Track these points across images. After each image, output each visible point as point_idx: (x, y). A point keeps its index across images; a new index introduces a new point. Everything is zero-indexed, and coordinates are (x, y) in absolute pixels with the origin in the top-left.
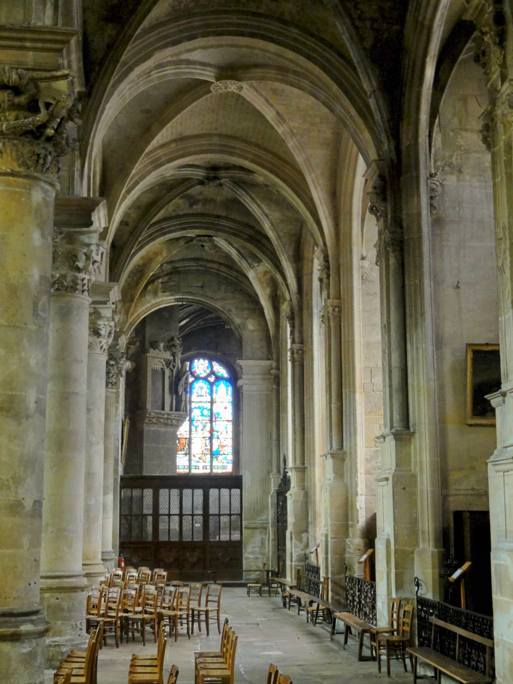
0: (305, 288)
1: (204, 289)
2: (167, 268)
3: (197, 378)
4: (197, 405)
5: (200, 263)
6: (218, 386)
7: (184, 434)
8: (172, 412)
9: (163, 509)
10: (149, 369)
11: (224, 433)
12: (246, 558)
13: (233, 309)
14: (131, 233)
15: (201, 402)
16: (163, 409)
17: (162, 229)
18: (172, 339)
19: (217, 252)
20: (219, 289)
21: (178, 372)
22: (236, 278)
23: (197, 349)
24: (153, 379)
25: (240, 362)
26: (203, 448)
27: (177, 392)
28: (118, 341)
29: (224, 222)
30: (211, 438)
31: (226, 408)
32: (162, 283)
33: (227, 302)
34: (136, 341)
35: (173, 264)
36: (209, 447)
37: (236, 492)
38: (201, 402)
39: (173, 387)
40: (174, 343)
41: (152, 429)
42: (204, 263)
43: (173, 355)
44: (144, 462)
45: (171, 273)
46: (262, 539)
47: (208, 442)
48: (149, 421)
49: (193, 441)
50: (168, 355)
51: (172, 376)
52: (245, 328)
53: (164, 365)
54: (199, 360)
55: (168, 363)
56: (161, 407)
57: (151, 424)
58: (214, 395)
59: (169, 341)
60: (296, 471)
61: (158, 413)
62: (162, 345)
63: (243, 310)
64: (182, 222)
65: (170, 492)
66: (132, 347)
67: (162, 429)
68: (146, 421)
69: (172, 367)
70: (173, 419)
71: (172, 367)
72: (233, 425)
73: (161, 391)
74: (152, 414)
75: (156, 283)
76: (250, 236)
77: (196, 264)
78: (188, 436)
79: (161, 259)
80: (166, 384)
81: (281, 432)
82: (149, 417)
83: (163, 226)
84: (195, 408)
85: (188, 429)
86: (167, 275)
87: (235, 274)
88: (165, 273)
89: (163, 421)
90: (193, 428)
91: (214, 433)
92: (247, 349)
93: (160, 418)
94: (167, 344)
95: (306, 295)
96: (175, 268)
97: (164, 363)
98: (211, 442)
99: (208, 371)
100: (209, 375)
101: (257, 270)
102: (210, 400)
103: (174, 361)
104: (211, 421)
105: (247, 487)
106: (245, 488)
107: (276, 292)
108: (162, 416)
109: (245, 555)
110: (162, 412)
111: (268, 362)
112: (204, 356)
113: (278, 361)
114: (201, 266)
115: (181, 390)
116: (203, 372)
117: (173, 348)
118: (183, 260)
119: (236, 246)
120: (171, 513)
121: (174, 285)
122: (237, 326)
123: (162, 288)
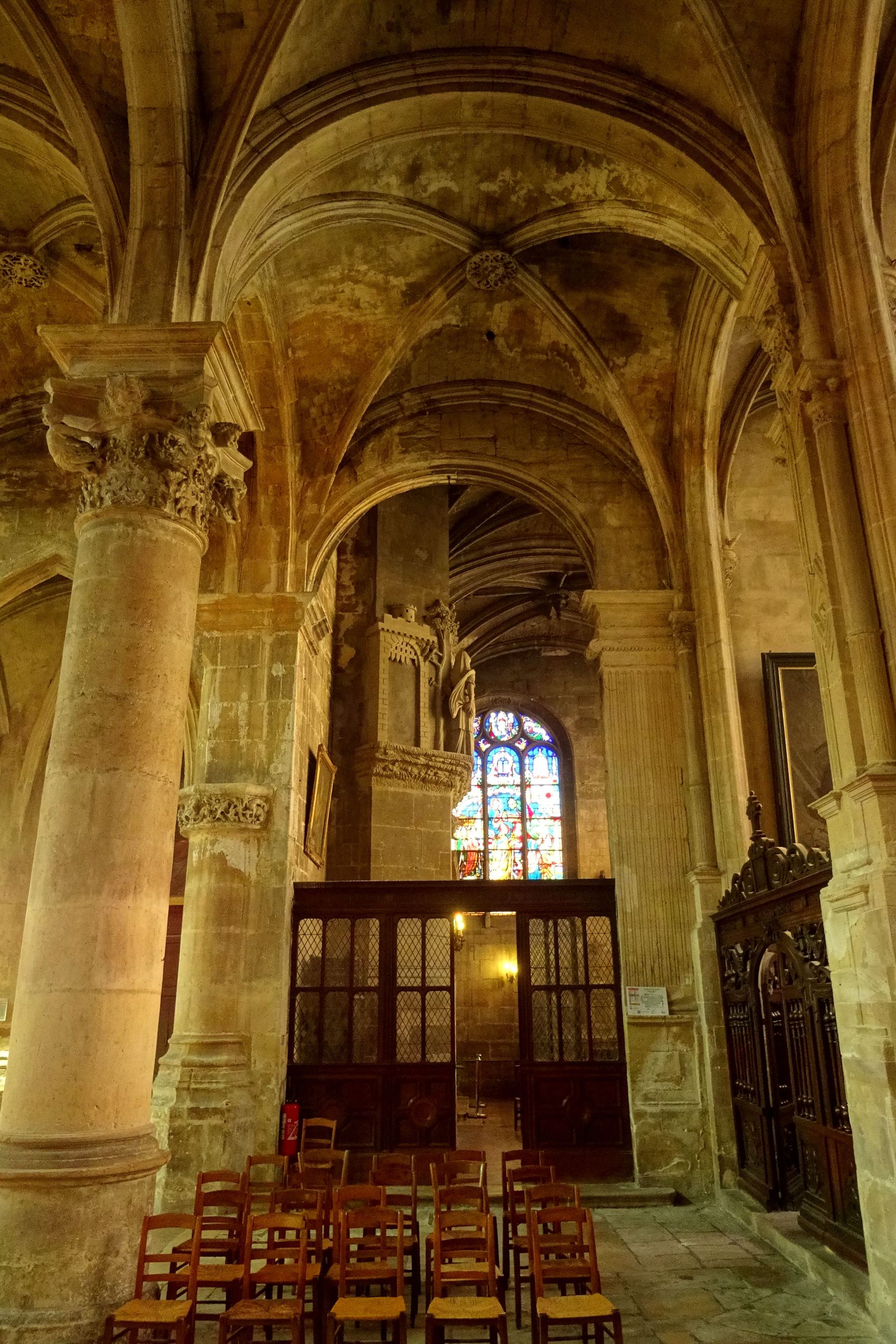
0: (824, 195)
1: (498, 443)
2: (412, 401)
3: (496, 743)
4: (497, 792)
5: (487, 388)
6: (533, 757)
7: (476, 844)
8: (436, 752)
9: (406, 976)
10: (383, 656)
11: (548, 841)
12: (640, 1115)
13: (569, 482)
14: (254, 48)
15: (504, 786)
16: (417, 743)
17: (360, 90)
18: (436, 603)
19: (524, 352)
20: (533, 442)
21: (450, 670)
22: (571, 418)
23: (493, 693)
24: (392, 678)
25: (590, 597)
26: (510, 869)
27: (446, 712)
28: (201, 361)
29: (544, 68)
30: (524, 851)
31: (548, 795)
32: (400, 434)
33: (552, 467)
34: (357, 603)
35: (426, 394)
36: (520, 867)
37: (597, 926)
38: (504, 786)
39: (439, 702)
40: (439, 610)
41: (392, 789)
42: (496, 389)
43: (439, 635)
44: (373, 865)
45: (422, 413)
46: (681, 1056)
47: (519, 856)
48: (384, 769)
49: (490, 856)
50: (425, 632)
51: (437, 680)
52: (600, 524)
53: (419, 653)
54: (497, 713)
55: (426, 650)
56: (413, 742)
57: (389, 777)
58: (527, 774)
59: (428, 608)
60: (879, 791)
61: (403, 751)
62: (412, 612)
63: (590, 483)
64: (419, 71)
65: (424, 926)
66: (347, 615)
67: (416, 792)
68: (378, 768)
69: (435, 661)
70: (440, 769)
71: (435, 661)
72: (562, 825)
73: (410, 708)
74: (391, 752)
75: (387, 435)
76: (628, 99)
77: (477, 392)
78: (482, 848)
79: (393, 356)
80: (422, 695)
81: (710, 759)
82: (383, 761)
83: (362, 83)
84: (494, 795)
85: (481, 835)
86: (412, 417)
87: (565, 408)
88: (407, 413)
89: (416, 771)
90: (491, 833)
91: (529, 841)
92: (606, 569)
93: (410, 763)
94: (424, 613)
95: (836, 209)
96: (430, 402)
97: (416, 647)
98: (524, 858)
99: (514, 732)
100: (517, 739)
101: (623, 375)
102: (518, 782)
103: (441, 649)
104: (522, 819)
105: (629, 911)
106: (625, 913)
107: (671, 433)
108: (414, 760)
109: (635, 1104)
110: (415, 750)
111: (661, 595)
112: (506, 706)
113: (687, 588)
114: (489, 396)
115: (455, 708)
116: (504, 733)
117: (439, 620)
118: (447, 383)
119: (571, 308)
120: (429, 983)
121: (429, 438)
122: (580, 520)
123: (403, 443)
